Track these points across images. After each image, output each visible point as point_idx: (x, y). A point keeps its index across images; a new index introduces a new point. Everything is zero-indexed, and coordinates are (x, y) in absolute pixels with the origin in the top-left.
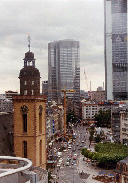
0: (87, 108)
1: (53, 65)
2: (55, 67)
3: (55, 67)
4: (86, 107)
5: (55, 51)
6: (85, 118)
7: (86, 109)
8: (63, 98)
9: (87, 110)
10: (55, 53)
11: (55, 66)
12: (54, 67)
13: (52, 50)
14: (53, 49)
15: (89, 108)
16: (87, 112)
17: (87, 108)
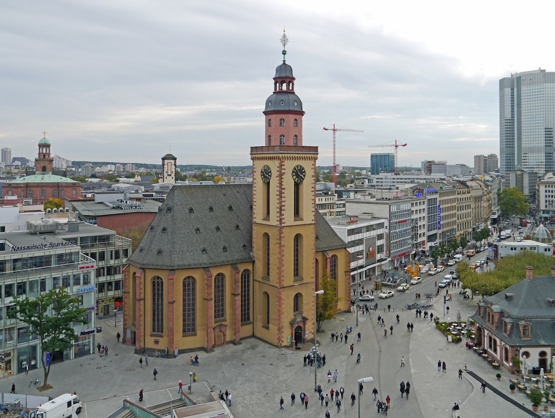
0: (548, 189)
1: (508, 116)
2: (512, 120)
3: (512, 120)
4: (546, 187)
5: (512, 93)
6: (542, 207)
7: (546, 191)
8: (519, 173)
9: (548, 194)
10: (512, 95)
11: (512, 117)
12: (510, 120)
13: (508, 91)
14: (510, 89)
15: (551, 189)
16: (546, 197)
17: (548, 189)
